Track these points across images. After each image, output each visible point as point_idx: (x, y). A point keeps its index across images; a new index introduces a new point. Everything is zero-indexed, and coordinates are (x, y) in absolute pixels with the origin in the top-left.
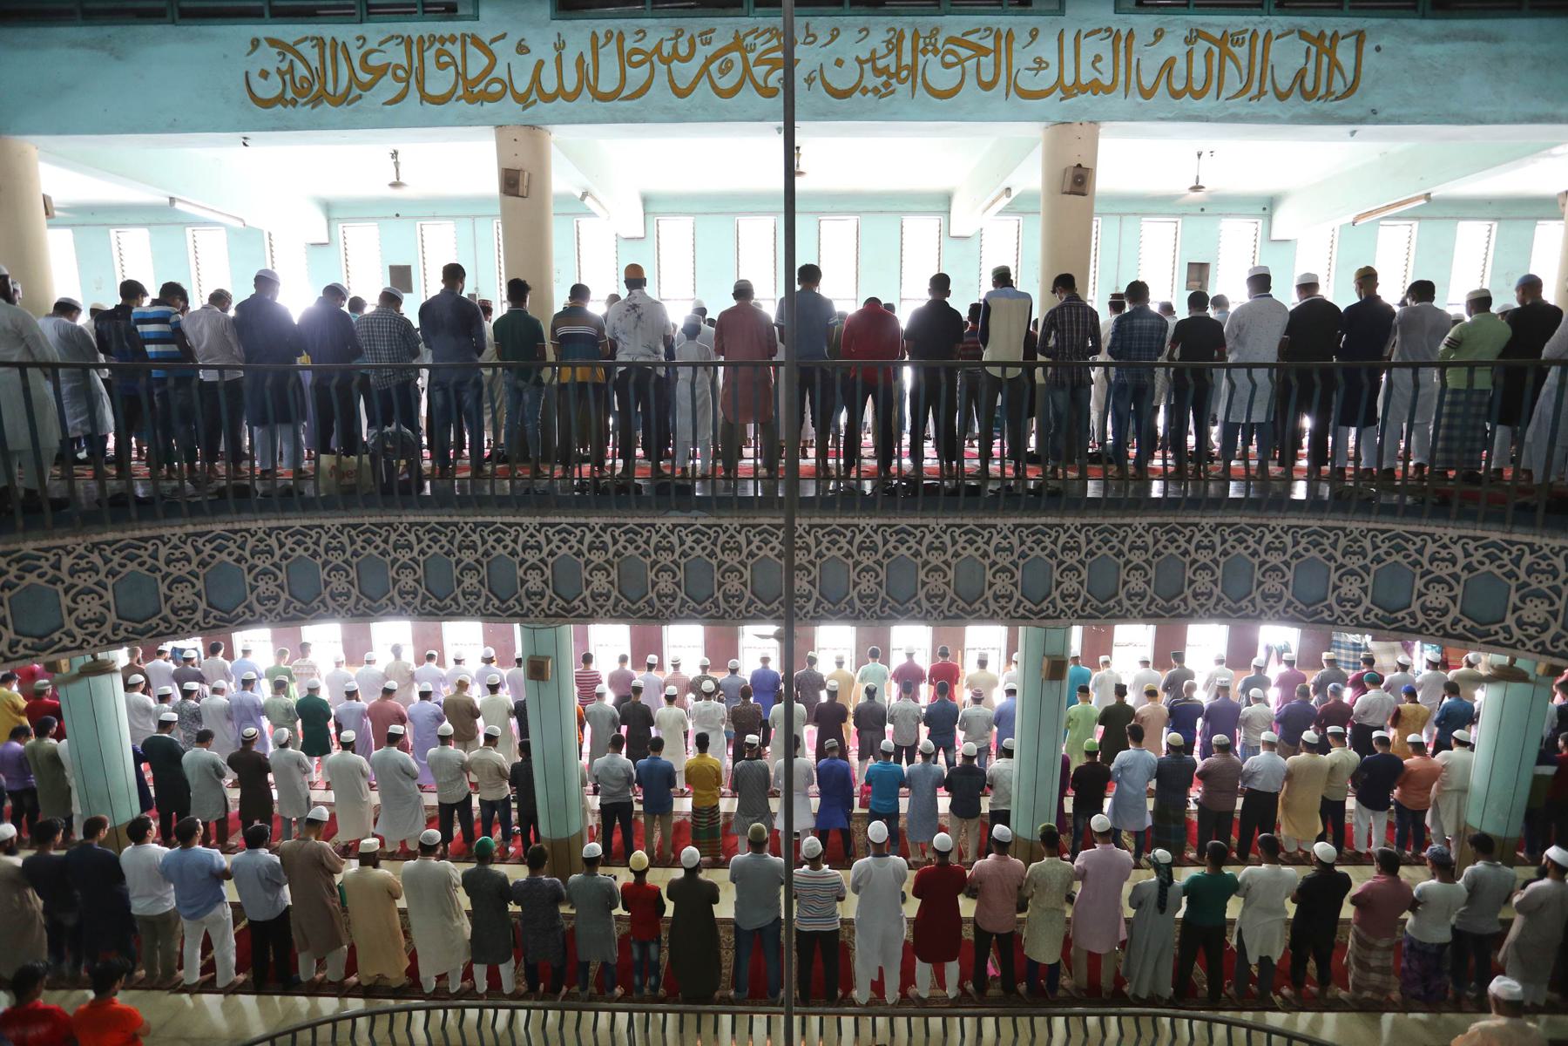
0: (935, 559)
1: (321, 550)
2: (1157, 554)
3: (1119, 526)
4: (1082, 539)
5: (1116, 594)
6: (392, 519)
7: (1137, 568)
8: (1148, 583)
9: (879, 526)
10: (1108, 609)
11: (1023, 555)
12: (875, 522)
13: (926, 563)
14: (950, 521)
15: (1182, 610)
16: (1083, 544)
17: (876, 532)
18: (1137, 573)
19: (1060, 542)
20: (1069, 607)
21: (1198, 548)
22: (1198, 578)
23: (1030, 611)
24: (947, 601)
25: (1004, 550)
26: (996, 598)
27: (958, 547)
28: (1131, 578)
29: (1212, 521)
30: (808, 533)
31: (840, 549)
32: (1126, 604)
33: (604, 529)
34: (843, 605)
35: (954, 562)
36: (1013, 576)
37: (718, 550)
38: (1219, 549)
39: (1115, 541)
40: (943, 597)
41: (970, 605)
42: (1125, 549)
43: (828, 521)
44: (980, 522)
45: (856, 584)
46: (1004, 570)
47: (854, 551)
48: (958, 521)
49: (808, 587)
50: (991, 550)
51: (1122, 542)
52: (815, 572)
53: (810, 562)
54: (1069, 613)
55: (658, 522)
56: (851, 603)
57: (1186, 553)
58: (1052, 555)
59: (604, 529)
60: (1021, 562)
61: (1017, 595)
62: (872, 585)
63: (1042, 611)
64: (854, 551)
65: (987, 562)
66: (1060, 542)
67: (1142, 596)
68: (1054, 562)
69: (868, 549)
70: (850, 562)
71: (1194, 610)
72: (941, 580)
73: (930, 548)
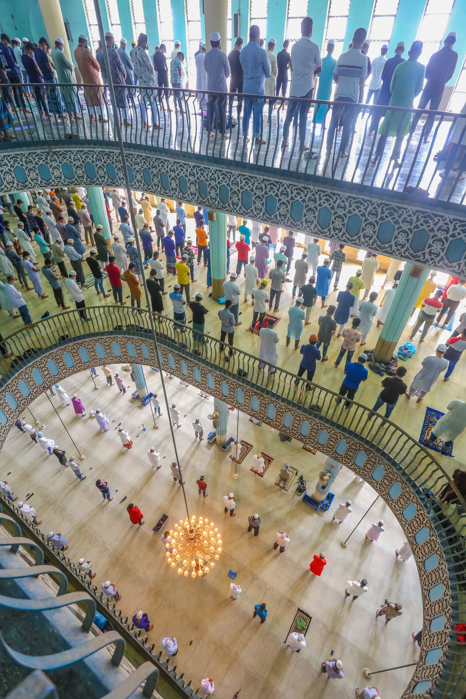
0: (311, 205)
1: (114, 161)
2: (417, 227)
3: (400, 208)
4: (379, 210)
5: (390, 242)
6: (133, 153)
7: (404, 231)
8: (408, 240)
9: (290, 185)
10: (385, 248)
11: (350, 212)
12: (288, 182)
13: (307, 206)
14: (320, 188)
15: (421, 258)
16: (380, 213)
17: (288, 187)
18: (403, 235)
19: (368, 210)
20: (366, 242)
21: (439, 229)
22: (434, 245)
23: (348, 239)
24: (314, 225)
25: (341, 207)
26: (334, 229)
27: (322, 201)
28: (400, 236)
29: (452, 217)
30: (263, 182)
31: (274, 192)
32: (394, 248)
33: (194, 167)
34: (273, 217)
35: (319, 208)
36: (343, 221)
37: (230, 183)
38: (451, 233)
39: (396, 215)
40: (312, 223)
41: (323, 229)
42: (400, 220)
43: (270, 179)
44: (333, 191)
45: (279, 209)
46: (339, 217)
47: (279, 194)
48: (323, 189)
49: (261, 206)
50: (336, 206)
51: (400, 217)
52: (264, 200)
53: (262, 195)
54: (366, 245)
55: (211, 168)
56: (276, 216)
57: (432, 230)
58: (363, 215)
59: (194, 167)
60: (348, 215)
61: (344, 230)
62: (285, 211)
63: (353, 240)
64: (279, 194)
65: (333, 212)
66: (368, 210)
67: (403, 246)
68: (363, 219)
69: (284, 194)
70: (277, 198)
71: (427, 260)
72: (312, 215)
73: (310, 199)
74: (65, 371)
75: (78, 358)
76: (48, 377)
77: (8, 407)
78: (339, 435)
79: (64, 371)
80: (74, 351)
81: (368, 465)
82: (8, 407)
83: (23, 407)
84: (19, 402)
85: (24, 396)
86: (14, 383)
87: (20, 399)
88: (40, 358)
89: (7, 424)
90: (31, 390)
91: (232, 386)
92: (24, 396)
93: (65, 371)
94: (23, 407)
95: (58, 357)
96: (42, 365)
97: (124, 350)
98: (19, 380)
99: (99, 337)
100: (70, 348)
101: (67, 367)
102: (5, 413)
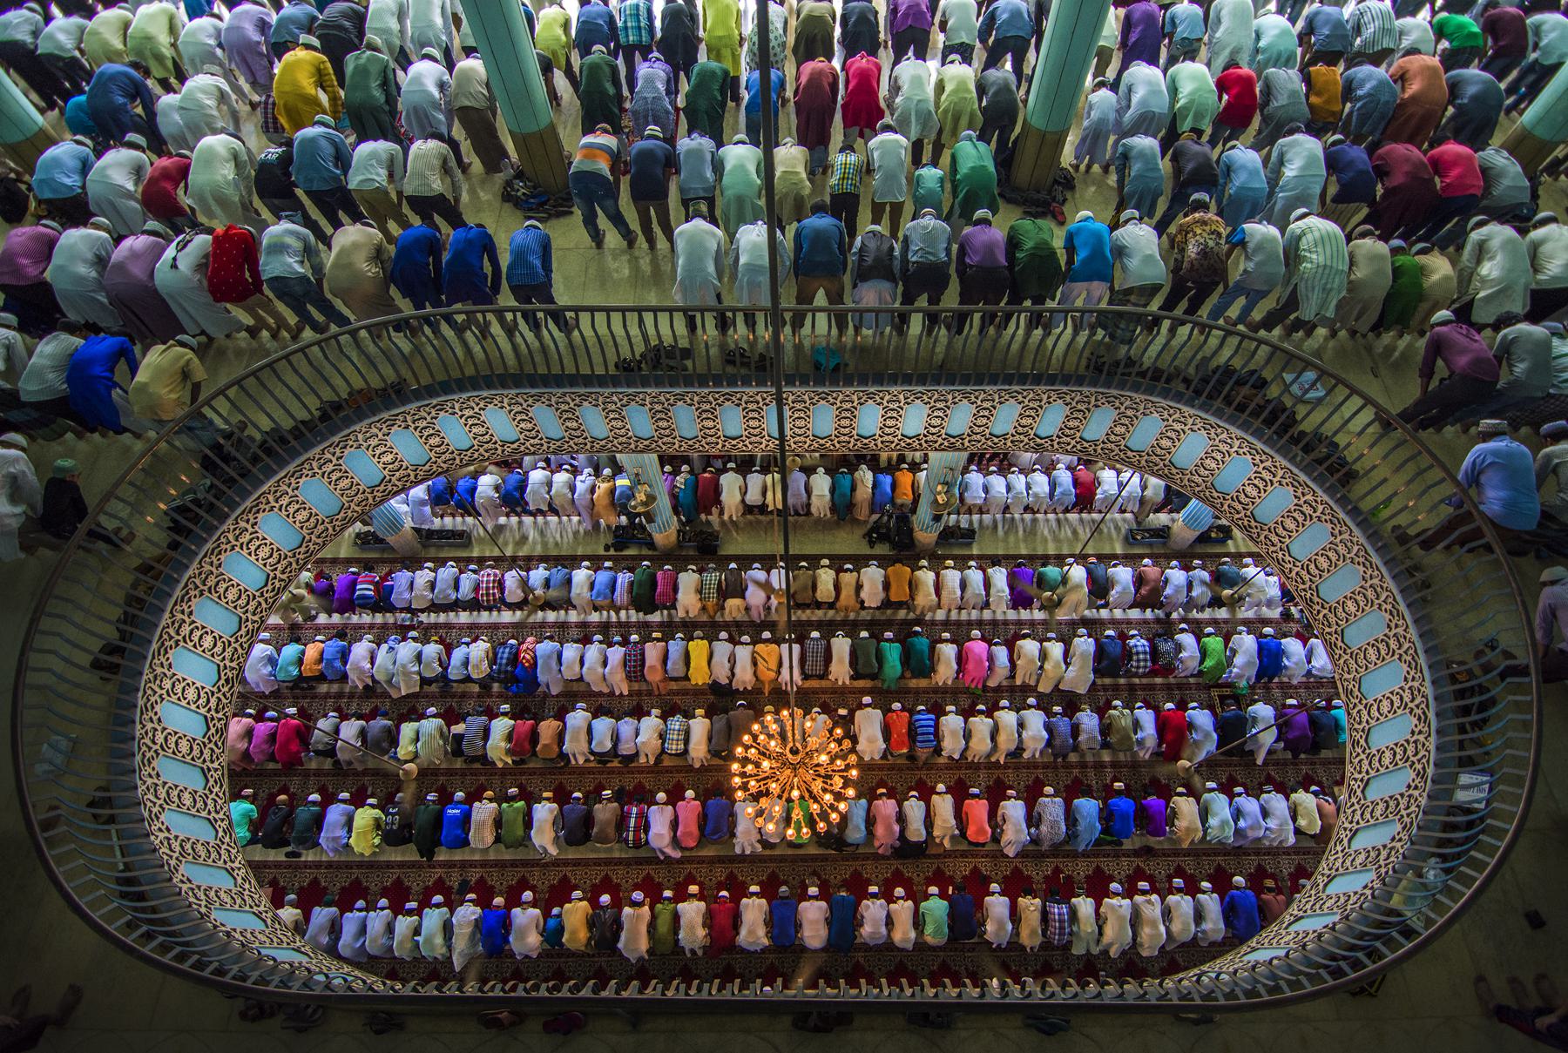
74: (253, 604)
75: (267, 549)
76: (218, 649)
77: (186, 795)
78: (1045, 397)
79: (251, 608)
80: (248, 537)
81: (1118, 430)
82: (186, 795)
83: (216, 765)
84: (199, 762)
85: (199, 737)
86: (149, 726)
87: (196, 752)
88: (167, 615)
89: (221, 834)
90: (203, 711)
91: (751, 406)
92: (199, 737)
93: (253, 604)
94: (216, 765)
95: (211, 581)
96: (186, 630)
97: (389, 458)
98: (157, 708)
99: (298, 461)
100: (231, 537)
101: (252, 590)
102: (193, 811)
